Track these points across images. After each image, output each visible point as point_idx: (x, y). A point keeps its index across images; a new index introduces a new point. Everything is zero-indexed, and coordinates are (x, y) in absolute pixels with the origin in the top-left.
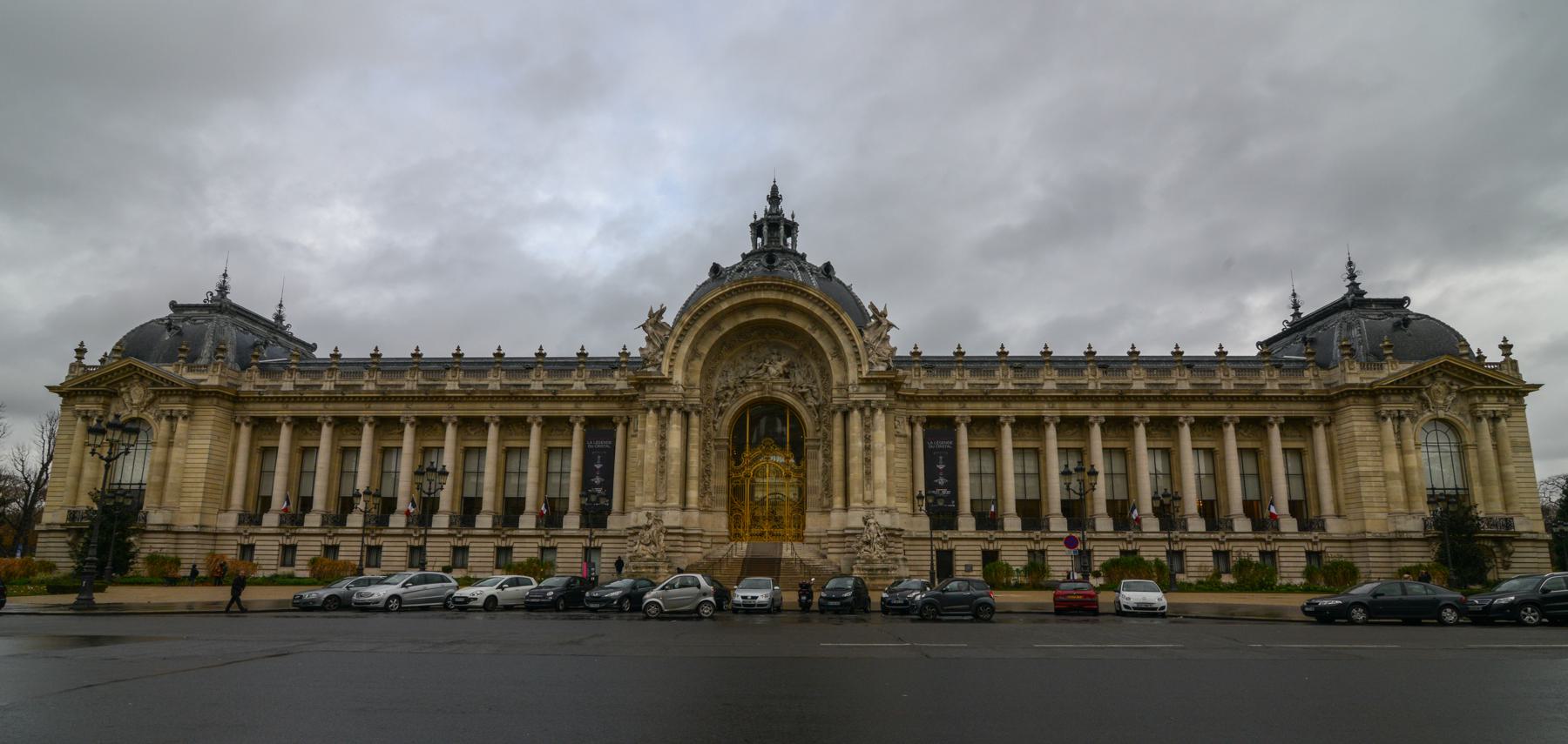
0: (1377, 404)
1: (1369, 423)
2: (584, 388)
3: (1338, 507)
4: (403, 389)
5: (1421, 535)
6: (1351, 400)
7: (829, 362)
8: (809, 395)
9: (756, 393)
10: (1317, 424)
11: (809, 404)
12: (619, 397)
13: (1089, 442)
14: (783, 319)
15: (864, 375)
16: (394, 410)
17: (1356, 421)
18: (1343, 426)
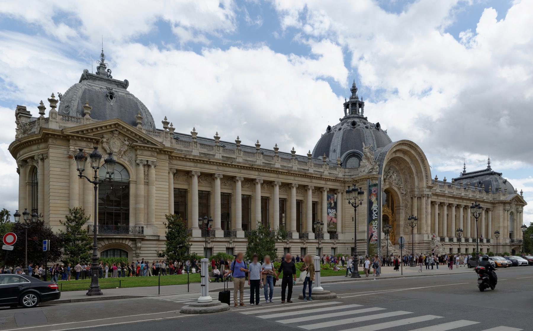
0: (504, 206)
1: (502, 212)
2: (328, 174)
3: (342, 230)
4: (256, 164)
5: (509, 244)
6: (500, 204)
7: (414, 177)
8: (401, 188)
9: (388, 186)
10: (490, 211)
11: (403, 192)
12: (342, 181)
13: (255, 192)
14: (403, 157)
15: (430, 185)
16: (253, 175)
17: (500, 210)
18: (496, 212)
